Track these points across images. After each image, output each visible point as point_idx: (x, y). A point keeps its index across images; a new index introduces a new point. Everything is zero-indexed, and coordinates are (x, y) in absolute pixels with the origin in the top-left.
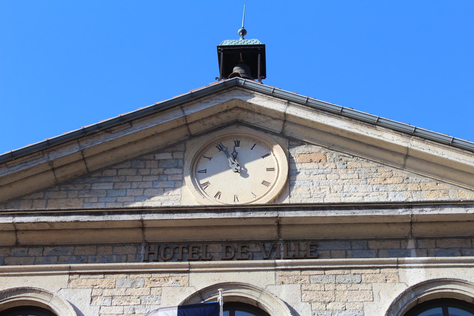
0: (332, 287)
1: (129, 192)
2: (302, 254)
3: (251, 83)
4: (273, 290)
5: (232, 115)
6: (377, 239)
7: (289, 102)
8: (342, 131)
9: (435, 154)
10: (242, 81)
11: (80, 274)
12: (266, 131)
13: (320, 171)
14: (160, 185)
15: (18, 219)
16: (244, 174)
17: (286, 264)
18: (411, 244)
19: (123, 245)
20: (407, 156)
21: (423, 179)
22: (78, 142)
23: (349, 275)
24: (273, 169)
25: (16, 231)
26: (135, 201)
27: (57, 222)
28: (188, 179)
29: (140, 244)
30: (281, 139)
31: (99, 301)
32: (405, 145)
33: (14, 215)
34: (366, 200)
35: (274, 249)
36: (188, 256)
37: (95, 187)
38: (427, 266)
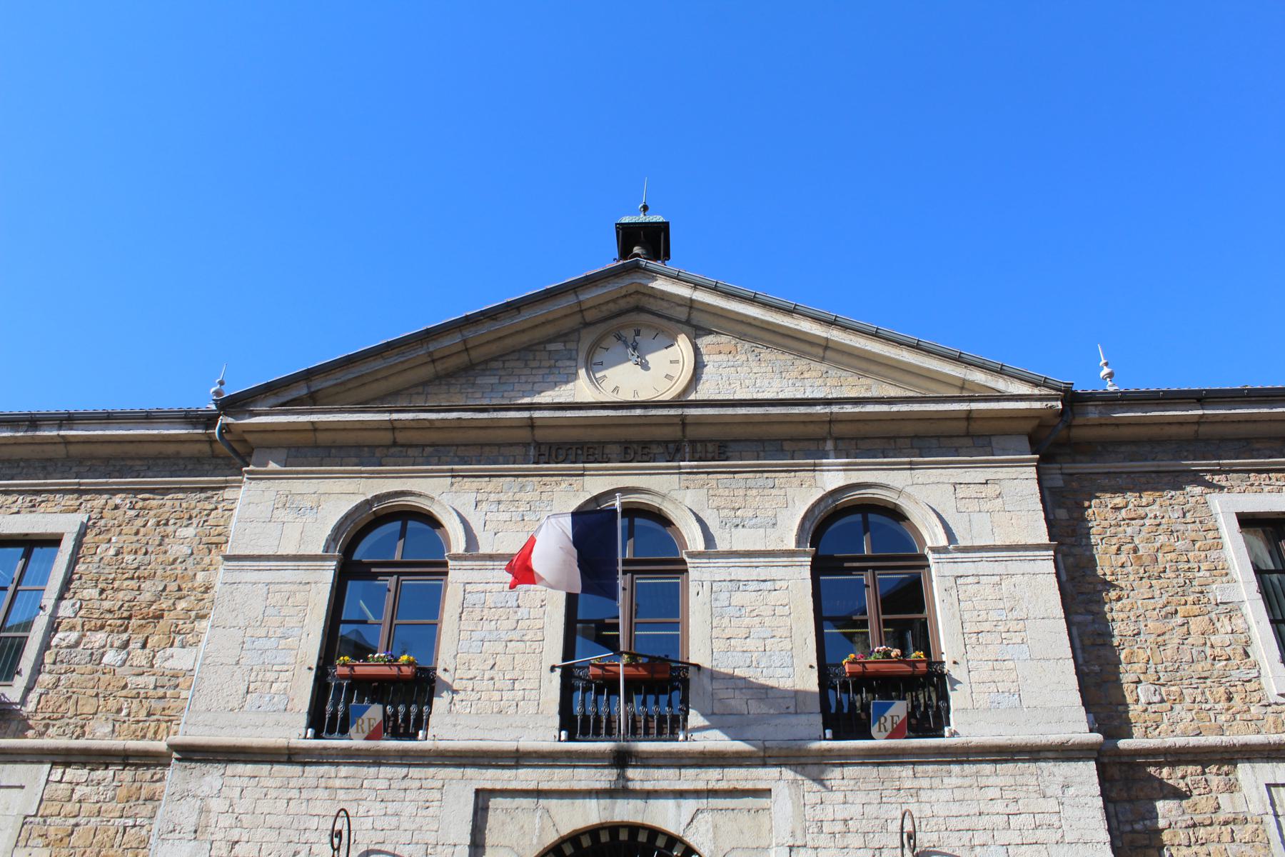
0: (742, 492)
1: (517, 387)
2: (709, 456)
3: (654, 265)
5: (632, 301)
6: (792, 439)
7: (696, 286)
8: (755, 319)
9: (857, 345)
10: (643, 262)
11: (464, 477)
12: (669, 319)
14: (551, 378)
15: (395, 416)
16: (645, 367)
17: (691, 467)
18: (829, 445)
19: (511, 445)
20: (826, 348)
21: (844, 374)
22: (460, 331)
23: (760, 479)
24: (677, 362)
25: (394, 429)
26: (523, 397)
27: (437, 420)
28: (582, 372)
29: (529, 444)
30: (686, 328)
31: (484, 506)
32: (824, 335)
33: (391, 412)
34: (781, 396)
35: (678, 450)
36: (582, 458)
37: (479, 381)
38: (847, 468)
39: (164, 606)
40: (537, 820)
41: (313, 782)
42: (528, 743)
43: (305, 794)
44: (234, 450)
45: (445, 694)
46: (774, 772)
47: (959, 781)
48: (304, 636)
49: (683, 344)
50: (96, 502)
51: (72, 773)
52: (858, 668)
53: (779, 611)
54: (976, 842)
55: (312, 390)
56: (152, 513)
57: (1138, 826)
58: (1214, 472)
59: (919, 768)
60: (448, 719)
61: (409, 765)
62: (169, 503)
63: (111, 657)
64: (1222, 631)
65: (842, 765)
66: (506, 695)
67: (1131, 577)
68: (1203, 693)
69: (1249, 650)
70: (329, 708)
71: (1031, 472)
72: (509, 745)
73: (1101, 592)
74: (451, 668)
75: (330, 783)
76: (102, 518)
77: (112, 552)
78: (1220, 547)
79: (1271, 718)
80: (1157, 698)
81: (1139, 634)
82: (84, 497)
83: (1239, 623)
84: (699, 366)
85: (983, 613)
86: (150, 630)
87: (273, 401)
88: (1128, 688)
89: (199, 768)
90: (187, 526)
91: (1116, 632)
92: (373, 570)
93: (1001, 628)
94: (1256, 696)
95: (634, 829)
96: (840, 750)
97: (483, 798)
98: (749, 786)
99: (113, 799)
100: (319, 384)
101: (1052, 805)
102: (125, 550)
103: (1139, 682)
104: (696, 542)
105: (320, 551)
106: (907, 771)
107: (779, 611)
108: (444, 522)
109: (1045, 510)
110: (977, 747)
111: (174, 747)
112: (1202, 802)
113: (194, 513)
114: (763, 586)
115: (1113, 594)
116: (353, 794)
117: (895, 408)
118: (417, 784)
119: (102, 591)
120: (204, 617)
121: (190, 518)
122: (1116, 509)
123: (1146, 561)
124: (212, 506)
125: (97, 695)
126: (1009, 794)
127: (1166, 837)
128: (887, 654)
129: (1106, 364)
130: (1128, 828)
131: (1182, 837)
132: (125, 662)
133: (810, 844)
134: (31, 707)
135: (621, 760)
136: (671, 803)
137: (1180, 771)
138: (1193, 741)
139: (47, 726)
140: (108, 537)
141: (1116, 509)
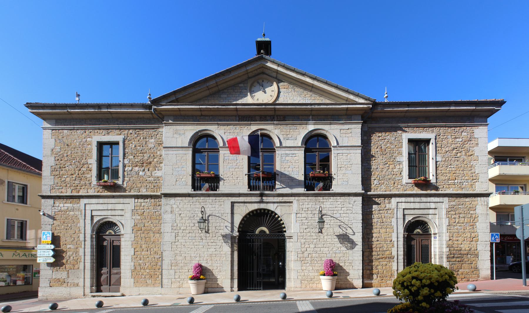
0: (289, 130)
1: (232, 98)
2: (281, 120)
3: (267, 57)
4: (273, 131)
8: (294, 77)
9: (321, 86)
10: (264, 56)
11: (221, 125)
12: (271, 77)
13: (287, 92)
14: (241, 96)
15: (201, 107)
16: (265, 92)
17: (277, 123)
18: (311, 117)
19: (232, 116)
20: (312, 87)
21: (316, 96)
22: (215, 79)
23: (293, 127)
24: (273, 91)
25: (201, 111)
26: (234, 101)
27: (212, 108)
28: (249, 94)
29: (236, 116)
30: (276, 80)
31: (226, 134)
33: (199, 105)
34: (300, 102)
35: (273, 118)
36: (250, 120)
37: (222, 96)
38: (315, 124)
39: (151, 160)
40: (244, 208)
41: (195, 201)
42: (241, 192)
43: (194, 204)
44: (159, 116)
45: (222, 181)
46: (293, 198)
47: (332, 200)
48: (187, 167)
49: (275, 84)
50: (125, 132)
51: (140, 200)
52: (313, 175)
53: (296, 161)
54: (334, 213)
55: (177, 98)
56: (141, 135)
57: (368, 210)
58: (406, 127)
59: (324, 197)
60: (224, 186)
61: (216, 197)
62: (145, 132)
63: (141, 173)
64: (397, 168)
65: (308, 197)
66: (236, 181)
67: (379, 155)
68: (389, 182)
69: (402, 173)
70: (196, 184)
71: (360, 126)
72: (237, 192)
73: (371, 158)
74: (223, 175)
75: (199, 201)
76: (128, 137)
77: (134, 146)
78: (402, 147)
79: (402, 188)
80: (379, 183)
81: (377, 168)
82: (122, 131)
83: (401, 166)
84: (279, 92)
85: (343, 163)
86: (149, 166)
87: (166, 101)
88: (372, 181)
89: (169, 199)
90: (152, 139)
91: (372, 168)
92: (201, 151)
93: (346, 166)
94: (400, 183)
95: (265, 210)
96: (308, 193)
97: (233, 204)
98: (288, 201)
99: (151, 206)
100: (179, 96)
101: (351, 206)
102: (137, 146)
103: (375, 179)
104: (277, 144)
105: (187, 146)
106: (321, 198)
107: (296, 161)
108: (217, 138)
109: (361, 137)
110: (337, 193)
111: (162, 194)
112: (383, 206)
113: (153, 135)
114: (293, 155)
115: (373, 159)
116: (205, 203)
117: (328, 107)
118: (218, 201)
119: (134, 157)
120: (162, 163)
121: (152, 137)
122: (379, 137)
123: (383, 150)
124: (157, 133)
125: (140, 182)
126: (342, 203)
127: (373, 212)
128: (320, 172)
129: (386, 93)
130: (366, 211)
131: (377, 212)
132: (145, 174)
133: (300, 213)
134: (125, 186)
135: (262, 195)
136: (272, 204)
137: (379, 199)
138: (384, 193)
139: (130, 190)
140: (131, 142)
141: (379, 137)
